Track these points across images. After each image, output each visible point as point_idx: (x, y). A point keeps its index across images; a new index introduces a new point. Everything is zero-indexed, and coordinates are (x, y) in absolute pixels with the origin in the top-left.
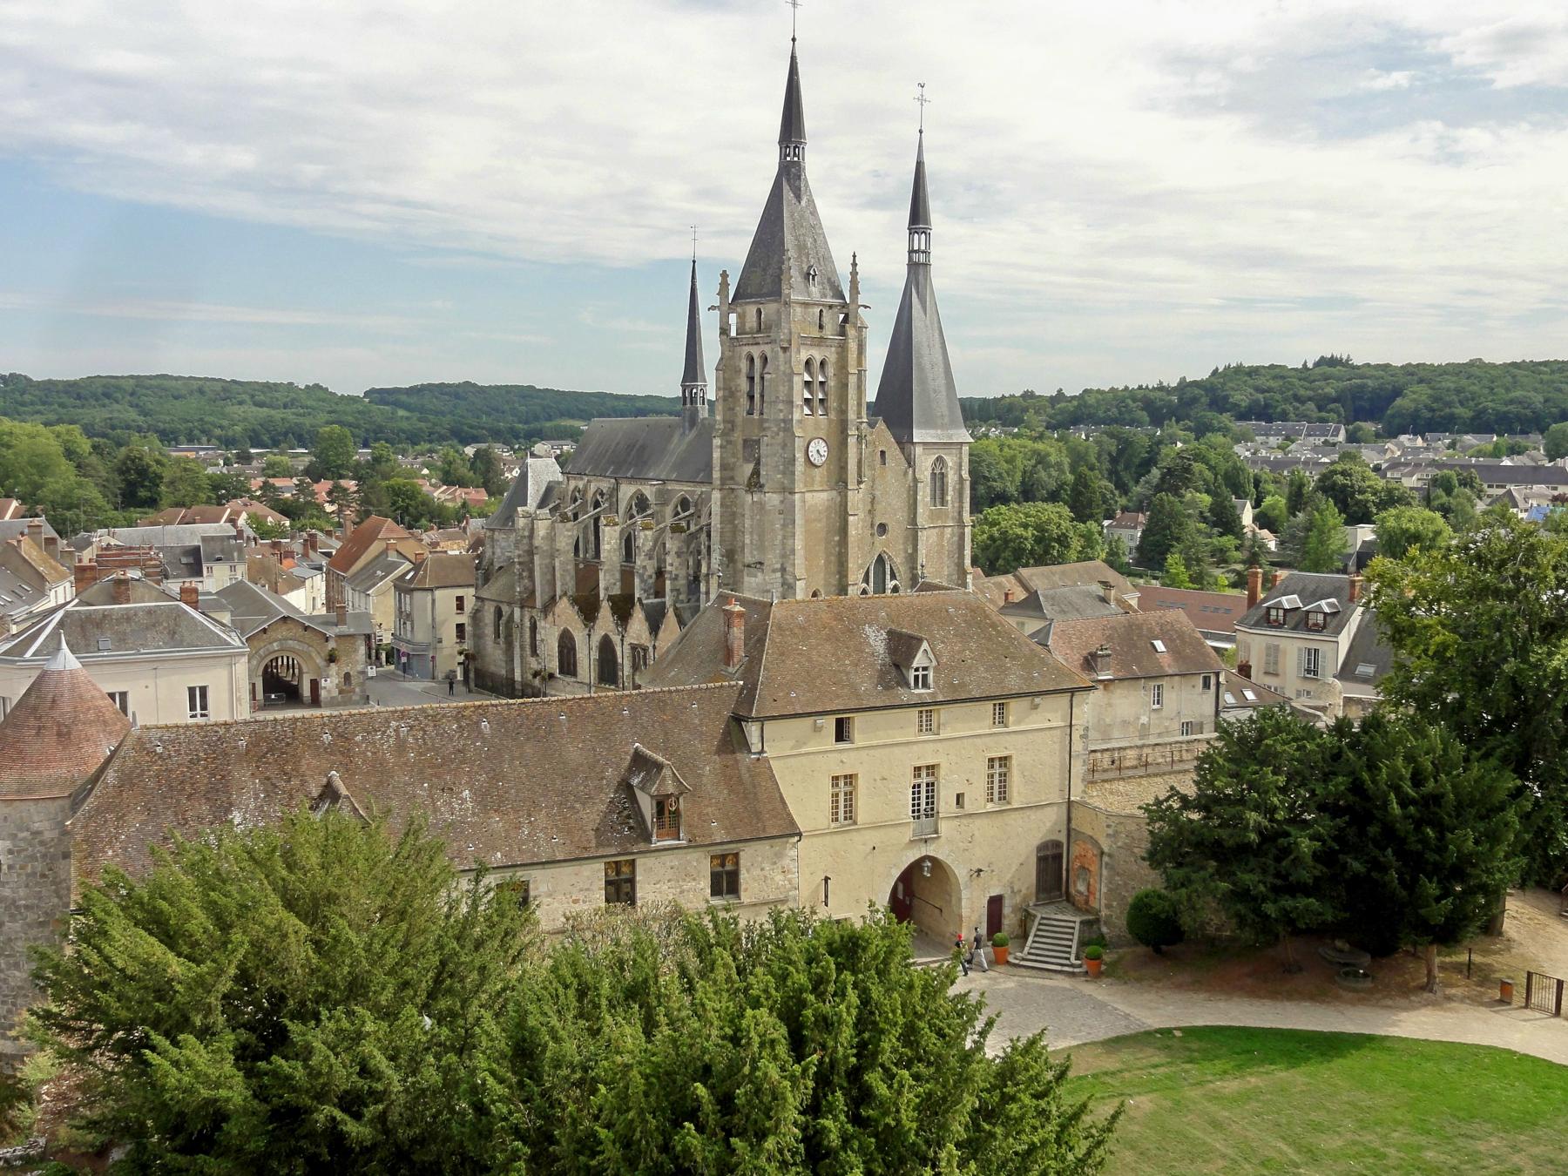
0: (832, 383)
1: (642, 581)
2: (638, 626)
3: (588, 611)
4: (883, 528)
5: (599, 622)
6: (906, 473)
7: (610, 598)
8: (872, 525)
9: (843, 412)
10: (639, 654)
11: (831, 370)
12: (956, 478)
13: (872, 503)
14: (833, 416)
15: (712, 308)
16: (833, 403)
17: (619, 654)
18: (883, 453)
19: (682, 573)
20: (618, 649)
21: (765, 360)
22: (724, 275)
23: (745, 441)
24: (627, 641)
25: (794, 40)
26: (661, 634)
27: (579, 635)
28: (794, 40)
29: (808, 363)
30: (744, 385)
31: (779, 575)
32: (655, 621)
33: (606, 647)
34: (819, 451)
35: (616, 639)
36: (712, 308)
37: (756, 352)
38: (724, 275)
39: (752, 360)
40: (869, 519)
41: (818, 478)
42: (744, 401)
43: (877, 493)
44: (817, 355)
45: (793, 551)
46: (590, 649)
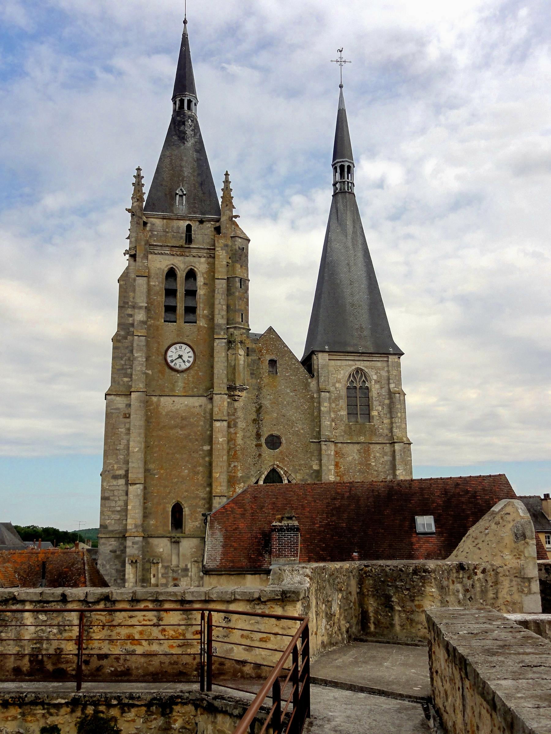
0: (201, 292)
4: (274, 442)
6: (307, 386)
8: (258, 436)
9: (211, 318)
11: (200, 281)
12: (384, 392)
13: (259, 410)
14: (202, 323)
16: (202, 311)
18: (273, 363)
25: (185, 22)
28: (185, 22)
29: (171, 274)
31: (122, 482)
34: (181, 356)
40: (253, 430)
41: (180, 384)
43: (266, 403)
44: (181, 265)
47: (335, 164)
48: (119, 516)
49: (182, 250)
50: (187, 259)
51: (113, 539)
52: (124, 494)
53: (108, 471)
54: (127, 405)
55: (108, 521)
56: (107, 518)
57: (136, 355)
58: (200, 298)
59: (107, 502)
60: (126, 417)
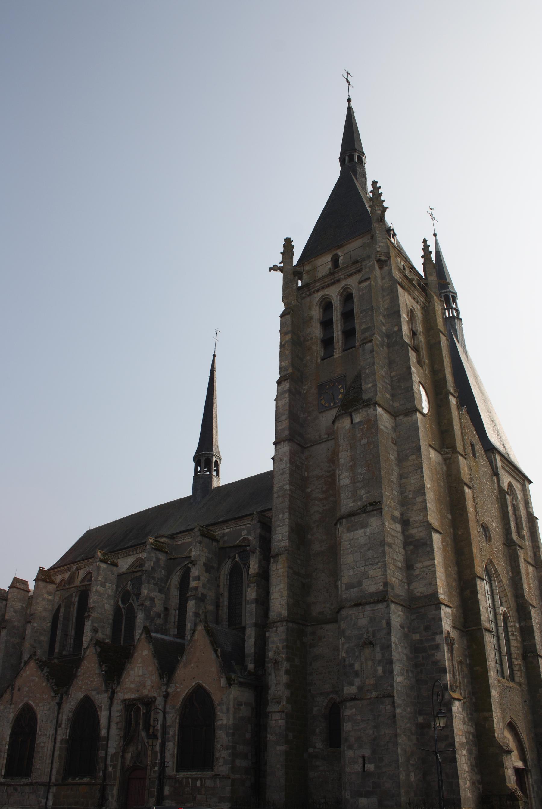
1: (148, 617)
2: (140, 674)
3: (61, 675)
5: (78, 682)
7: (98, 643)
10: (138, 712)
15: (274, 268)
17: (103, 721)
19: (211, 595)
20: (103, 716)
21: (348, 298)
22: (288, 245)
23: (321, 388)
24: (121, 695)
26: (181, 673)
27: (44, 712)
30: (316, 331)
32: (168, 660)
33: (86, 711)
35: (101, 699)
36: (274, 268)
37: (334, 293)
38: (288, 245)
39: (327, 306)
42: (318, 349)
45: (421, 490)
46: (58, 725)
47: (446, 292)
48: (401, 576)
49: (410, 285)
50: (410, 297)
51: (400, 608)
52: (401, 545)
53: (388, 508)
54: (392, 427)
55: (394, 579)
56: (392, 574)
57: (413, 369)
58: (422, 344)
59: (391, 550)
60: (393, 443)
